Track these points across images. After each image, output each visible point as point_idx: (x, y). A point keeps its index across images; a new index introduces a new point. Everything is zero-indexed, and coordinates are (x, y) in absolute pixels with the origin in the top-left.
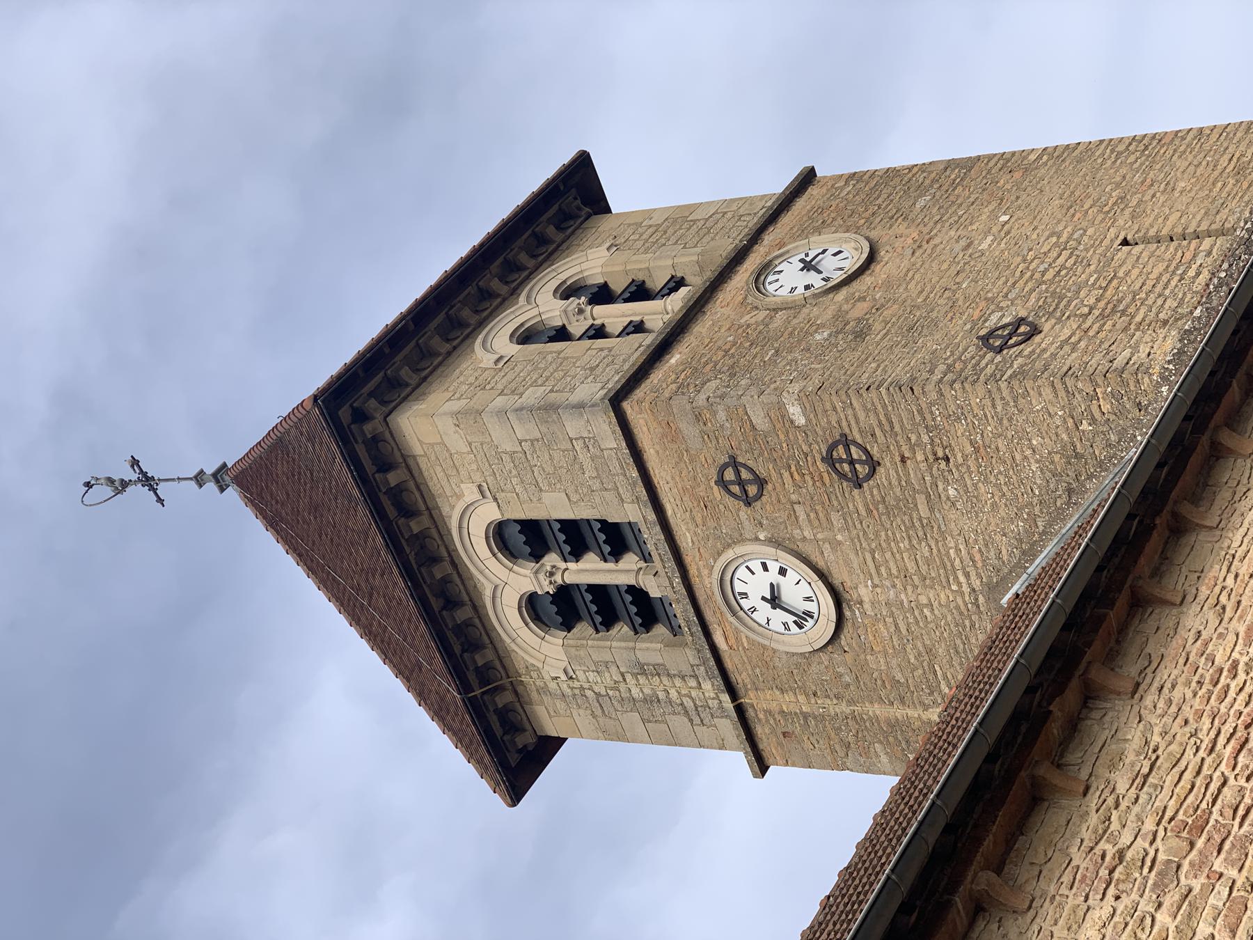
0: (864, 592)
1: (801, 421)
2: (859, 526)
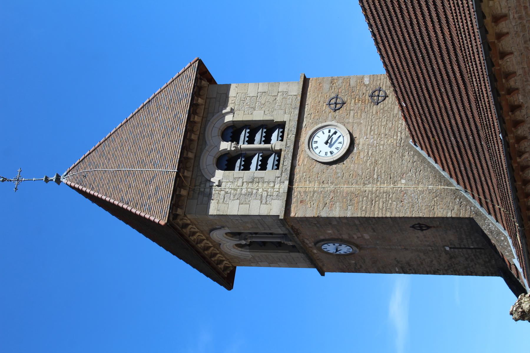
0: (362, 141)
2: (371, 117)
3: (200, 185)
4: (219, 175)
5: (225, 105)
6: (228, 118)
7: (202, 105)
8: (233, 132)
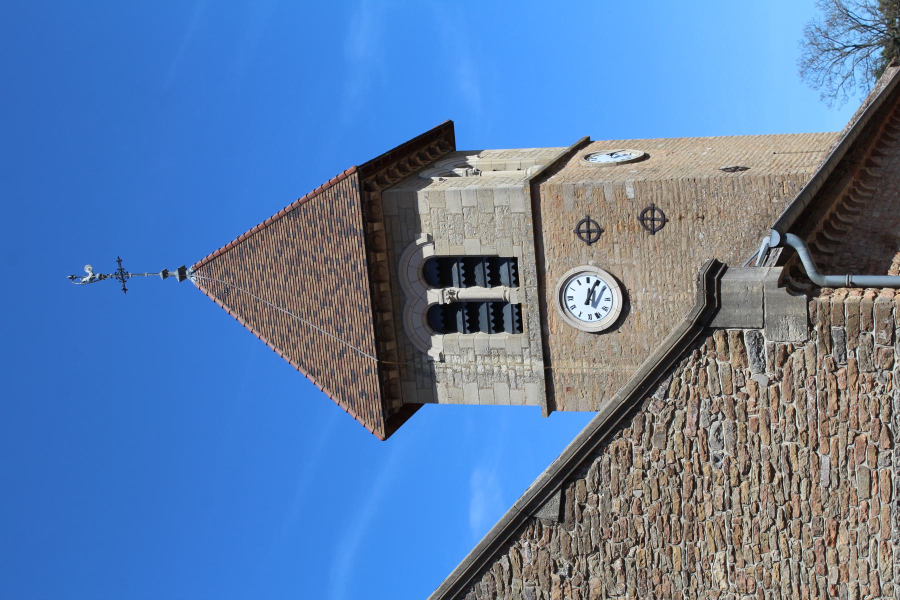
1: (631, 195)
2: (647, 256)
3: (413, 359)
4: (438, 343)
5: (417, 230)
6: (428, 252)
8: (439, 271)
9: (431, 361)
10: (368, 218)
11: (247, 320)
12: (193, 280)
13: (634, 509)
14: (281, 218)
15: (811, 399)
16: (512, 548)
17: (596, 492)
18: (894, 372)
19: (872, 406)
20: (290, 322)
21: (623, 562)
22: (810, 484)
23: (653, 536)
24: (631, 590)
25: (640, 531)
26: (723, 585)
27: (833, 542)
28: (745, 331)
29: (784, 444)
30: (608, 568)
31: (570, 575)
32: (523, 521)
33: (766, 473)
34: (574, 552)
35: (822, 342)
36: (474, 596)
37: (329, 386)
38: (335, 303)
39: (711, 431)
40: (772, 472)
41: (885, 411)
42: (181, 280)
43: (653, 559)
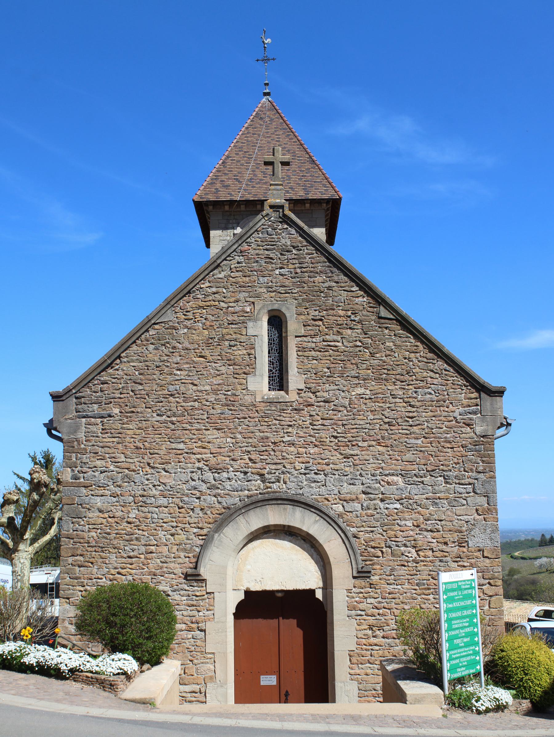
3: (234, 219)
7: (305, 207)
9: (233, 228)
10: (313, 202)
11: (247, 128)
12: (264, 99)
13: (388, 353)
14: (308, 153)
15: (449, 436)
16: (362, 293)
17: (395, 335)
18: (463, 473)
19: (446, 463)
20: (251, 153)
21: (361, 346)
22: (407, 434)
23: (376, 361)
24: (346, 349)
25: (378, 355)
26: (353, 393)
27: (379, 444)
28: (479, 407)
29: (426, 423)
30: (357, 339)
31: (351, 320)
32: (378, 299)
33: (411, 415)
34: (364, 323)
35: (476, 441)
36: (336, 272)
37: (218, 171)
38: (266, 180)
39: (430, 390)
40: (412, 418)
41: (445, 468)
42: (264, 93)
43: (363, 361)
